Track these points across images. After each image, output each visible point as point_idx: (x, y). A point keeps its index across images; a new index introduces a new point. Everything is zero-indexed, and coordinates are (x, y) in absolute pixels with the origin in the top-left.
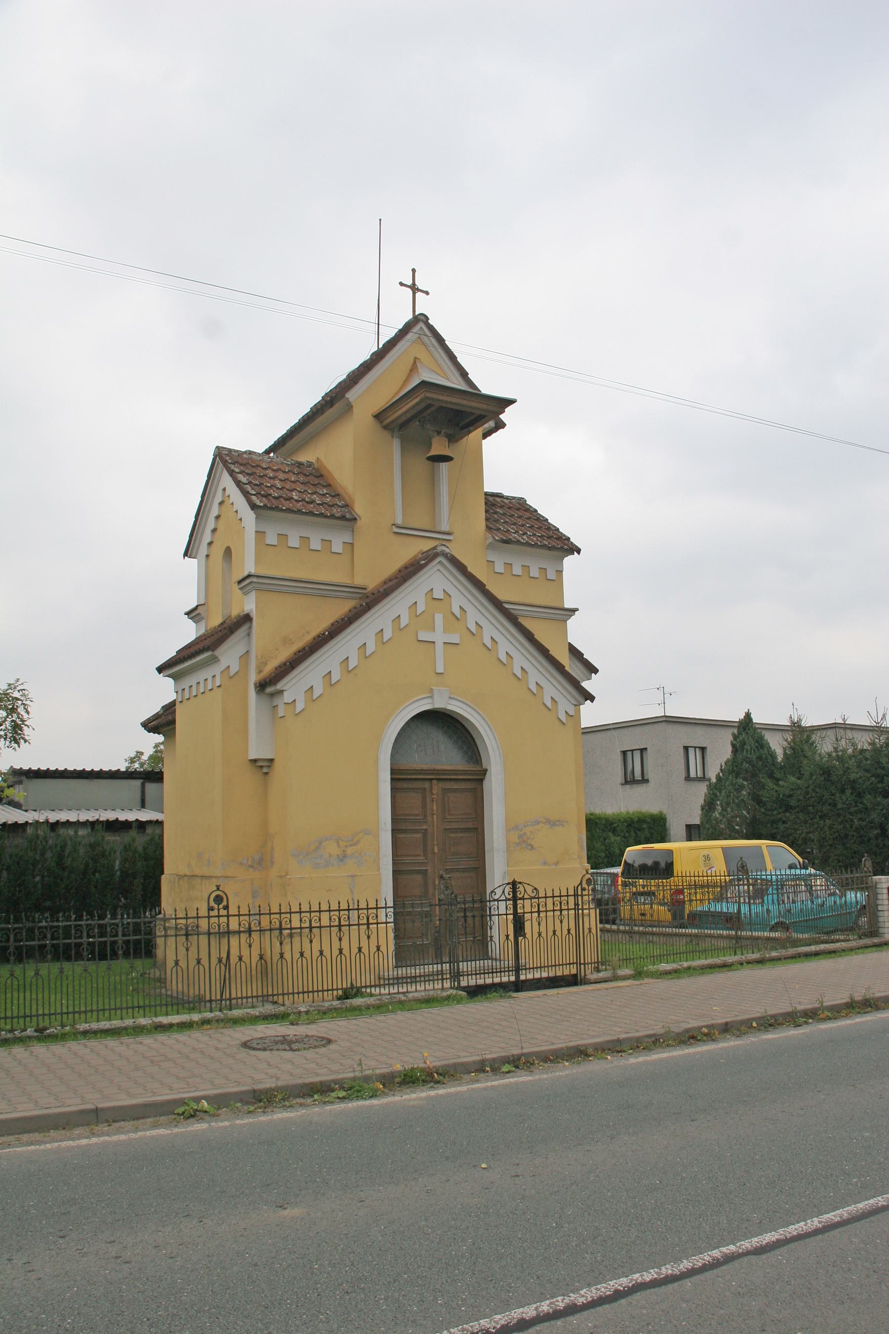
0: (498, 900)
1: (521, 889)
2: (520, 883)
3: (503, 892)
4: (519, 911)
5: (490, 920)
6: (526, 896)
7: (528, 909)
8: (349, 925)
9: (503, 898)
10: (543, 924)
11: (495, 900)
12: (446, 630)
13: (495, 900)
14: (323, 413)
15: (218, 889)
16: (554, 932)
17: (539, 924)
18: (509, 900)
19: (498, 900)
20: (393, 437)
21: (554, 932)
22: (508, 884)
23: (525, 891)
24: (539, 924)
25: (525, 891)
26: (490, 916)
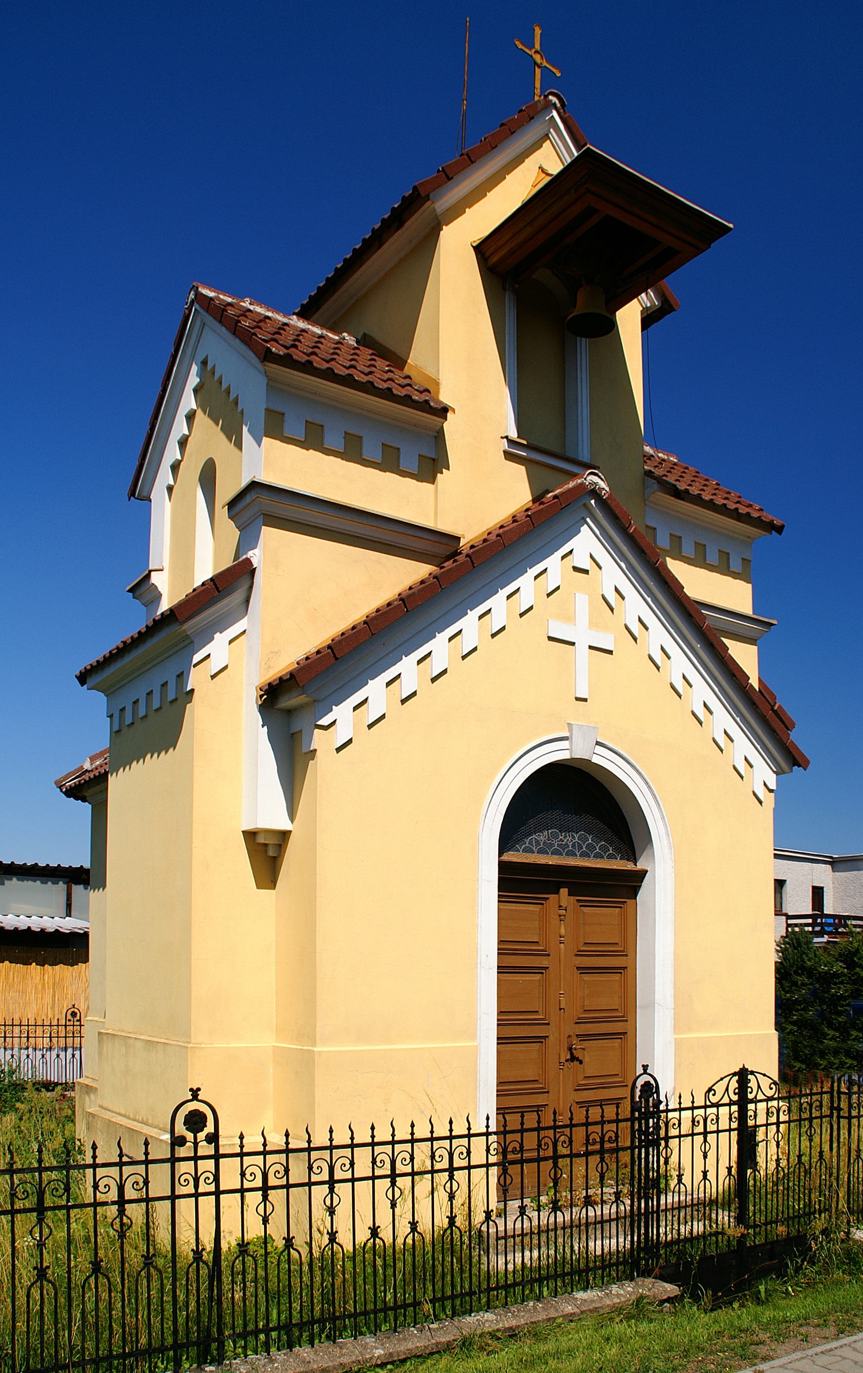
0: (717, 1105)
1: (753, 1084)
2: (752, 1073)
3: (727, 1089)
4: (751, 1123)
5: (667, 1146)
6: (760, 1096)
7: (761, 1120)
8: (469, 1167)
9: (726, 1100)
10: (712, 1155)
11: (713, 1105)
12: (594, 624)
13: (713, 1105)
14: (401, 226)
15: (645, 1072)
16: (705, 1173)
17: (705, 1157)
18: (734, 1103)
19: (717, 1105)
20: (504, 289)
21: (705, 1173)
22: (734, 1074)
23: (759, 1087)
24: (705, 1157)
25: (759, 1087)
26: (667, 1138)
